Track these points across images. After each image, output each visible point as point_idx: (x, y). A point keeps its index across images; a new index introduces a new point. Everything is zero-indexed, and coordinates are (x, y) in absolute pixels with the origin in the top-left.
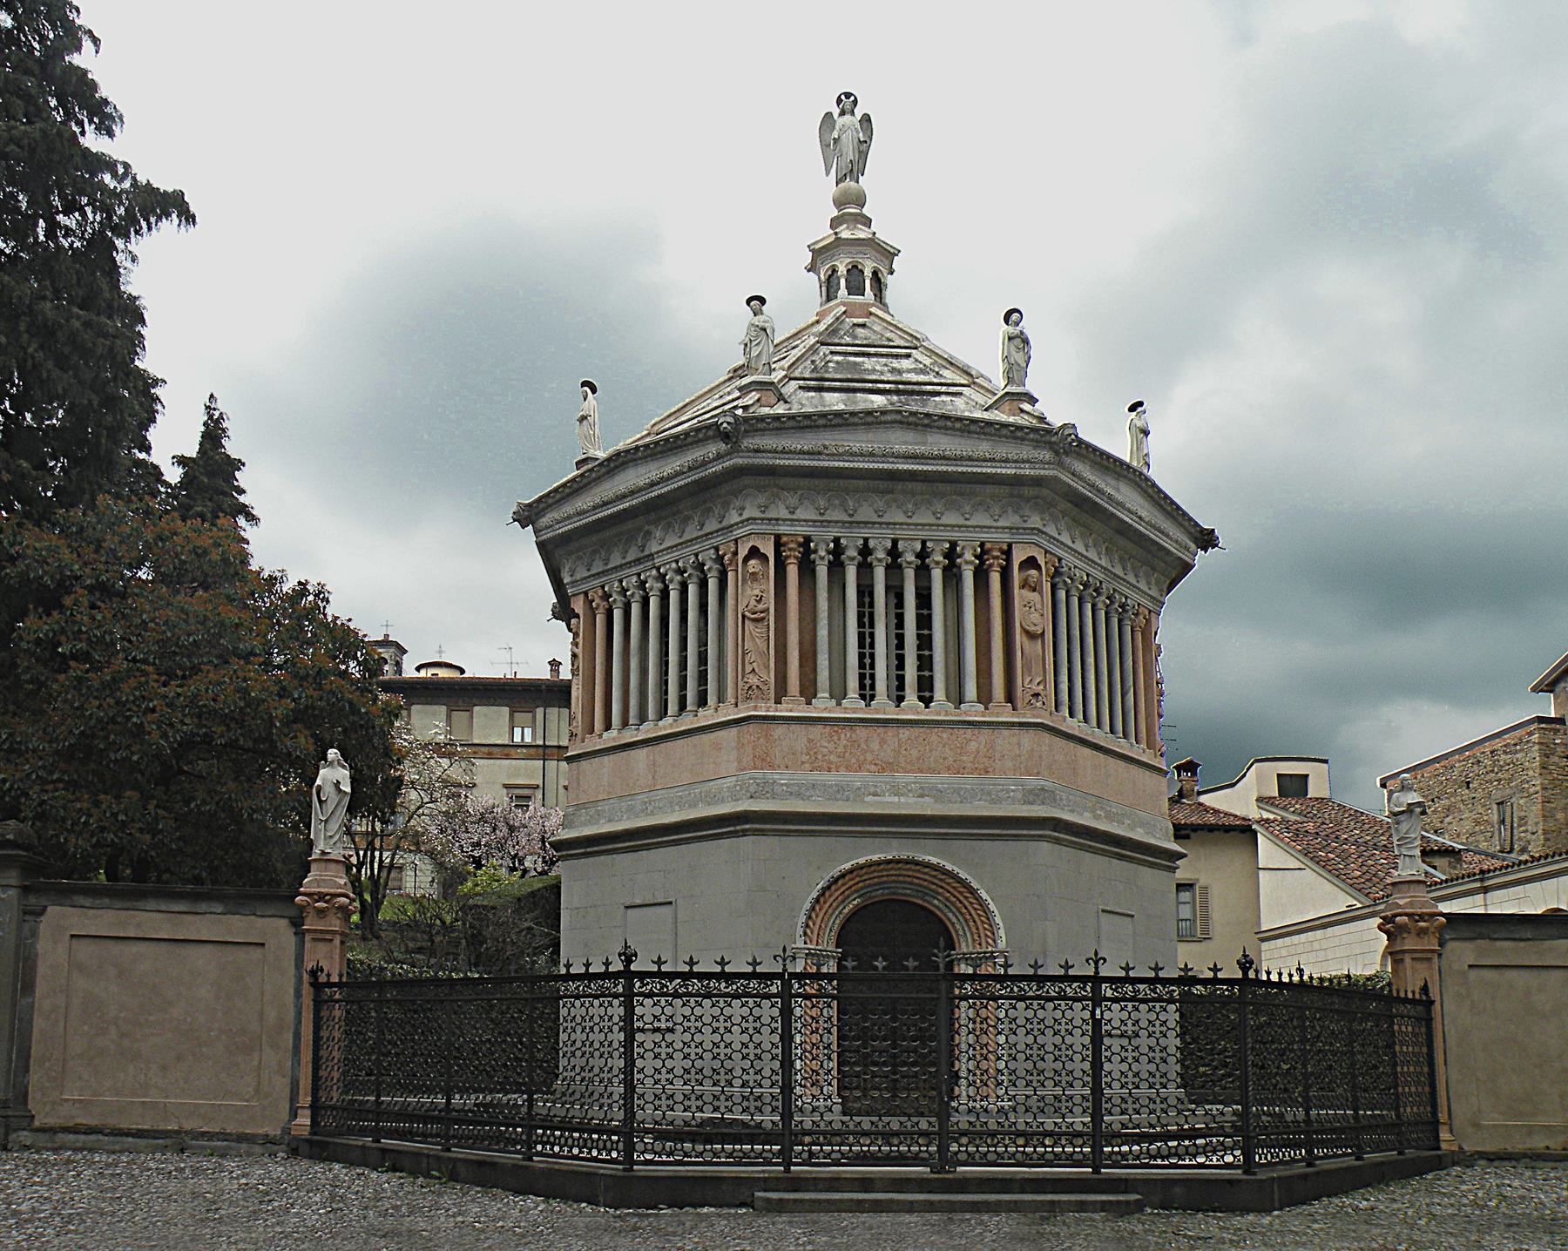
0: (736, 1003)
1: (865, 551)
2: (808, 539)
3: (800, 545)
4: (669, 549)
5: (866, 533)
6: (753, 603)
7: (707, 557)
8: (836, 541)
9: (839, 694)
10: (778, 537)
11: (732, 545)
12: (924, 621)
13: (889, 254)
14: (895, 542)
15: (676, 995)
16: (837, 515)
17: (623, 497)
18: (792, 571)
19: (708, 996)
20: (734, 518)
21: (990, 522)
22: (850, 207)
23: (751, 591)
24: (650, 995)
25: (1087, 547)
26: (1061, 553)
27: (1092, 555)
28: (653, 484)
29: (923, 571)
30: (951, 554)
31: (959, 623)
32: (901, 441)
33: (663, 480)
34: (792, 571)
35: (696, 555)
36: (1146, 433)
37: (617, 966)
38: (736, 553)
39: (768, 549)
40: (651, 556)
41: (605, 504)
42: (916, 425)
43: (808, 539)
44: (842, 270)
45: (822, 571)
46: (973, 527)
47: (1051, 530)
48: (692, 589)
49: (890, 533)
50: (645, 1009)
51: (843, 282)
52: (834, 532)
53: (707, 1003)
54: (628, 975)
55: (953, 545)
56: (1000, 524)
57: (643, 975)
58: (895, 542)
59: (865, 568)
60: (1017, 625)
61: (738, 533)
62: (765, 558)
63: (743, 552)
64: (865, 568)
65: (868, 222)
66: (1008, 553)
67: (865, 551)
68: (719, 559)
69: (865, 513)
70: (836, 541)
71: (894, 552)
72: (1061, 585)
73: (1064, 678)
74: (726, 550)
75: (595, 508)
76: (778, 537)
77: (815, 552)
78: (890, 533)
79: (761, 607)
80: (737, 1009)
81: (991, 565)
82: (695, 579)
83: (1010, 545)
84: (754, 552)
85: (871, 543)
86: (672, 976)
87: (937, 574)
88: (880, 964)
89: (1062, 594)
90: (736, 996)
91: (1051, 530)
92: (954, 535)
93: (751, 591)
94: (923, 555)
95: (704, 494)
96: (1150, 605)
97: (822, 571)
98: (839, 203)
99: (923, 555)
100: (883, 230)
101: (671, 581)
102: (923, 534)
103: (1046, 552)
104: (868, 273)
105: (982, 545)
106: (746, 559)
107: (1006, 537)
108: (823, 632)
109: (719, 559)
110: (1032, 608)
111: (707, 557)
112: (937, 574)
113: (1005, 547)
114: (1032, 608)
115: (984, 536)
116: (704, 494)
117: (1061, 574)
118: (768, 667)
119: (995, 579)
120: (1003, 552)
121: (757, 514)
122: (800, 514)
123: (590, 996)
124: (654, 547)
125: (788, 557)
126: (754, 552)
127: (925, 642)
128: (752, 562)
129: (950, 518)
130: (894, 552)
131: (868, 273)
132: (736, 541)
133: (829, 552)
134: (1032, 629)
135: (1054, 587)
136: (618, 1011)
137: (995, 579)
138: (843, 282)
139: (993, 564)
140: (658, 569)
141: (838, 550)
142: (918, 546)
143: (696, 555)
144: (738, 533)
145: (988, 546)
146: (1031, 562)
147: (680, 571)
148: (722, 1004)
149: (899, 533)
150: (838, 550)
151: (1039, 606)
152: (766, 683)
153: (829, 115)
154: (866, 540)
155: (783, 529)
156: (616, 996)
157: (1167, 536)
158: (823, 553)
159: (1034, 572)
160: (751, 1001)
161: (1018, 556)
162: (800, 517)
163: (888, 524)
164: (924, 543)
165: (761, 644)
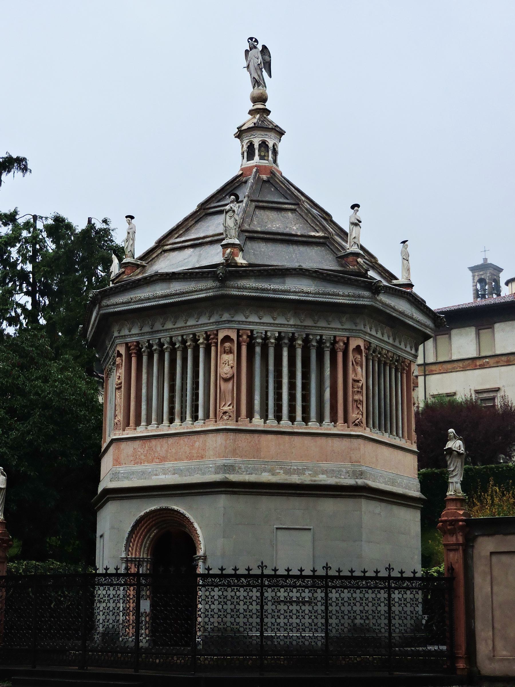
2: (138, 343)
5: (159, 335)
8: (148, 341)
10: (127, 344)
16: (146, 329)
18: (134, 360)
25: (274, 319)
26: (251, 327)
30: (195, 339)
34: (134, 360)
39: (122, 350)
45: (145, 359)
46: (199, 325)
52: (147, 337)
55: (194, 335)
56: (211, 321)
58: (171, 338)
76: (127, 344)
79: (119, 381)
83: (217, 331)
91: (240, 318)
94: (184, 342)
97: (145, 359)
98: (256, 100)
99: (184, 342)
102: (182, 332)
105: (206, 333)
117: (256, 338)
129: (191, 322)
134: (225, 376)
142: (180, 338)
145: (209, 333)
149: (173, 333)
150: (150, 346)
155: (128, 340)
157: (338, 295)
159: (227, 345)
164: (182, 336)
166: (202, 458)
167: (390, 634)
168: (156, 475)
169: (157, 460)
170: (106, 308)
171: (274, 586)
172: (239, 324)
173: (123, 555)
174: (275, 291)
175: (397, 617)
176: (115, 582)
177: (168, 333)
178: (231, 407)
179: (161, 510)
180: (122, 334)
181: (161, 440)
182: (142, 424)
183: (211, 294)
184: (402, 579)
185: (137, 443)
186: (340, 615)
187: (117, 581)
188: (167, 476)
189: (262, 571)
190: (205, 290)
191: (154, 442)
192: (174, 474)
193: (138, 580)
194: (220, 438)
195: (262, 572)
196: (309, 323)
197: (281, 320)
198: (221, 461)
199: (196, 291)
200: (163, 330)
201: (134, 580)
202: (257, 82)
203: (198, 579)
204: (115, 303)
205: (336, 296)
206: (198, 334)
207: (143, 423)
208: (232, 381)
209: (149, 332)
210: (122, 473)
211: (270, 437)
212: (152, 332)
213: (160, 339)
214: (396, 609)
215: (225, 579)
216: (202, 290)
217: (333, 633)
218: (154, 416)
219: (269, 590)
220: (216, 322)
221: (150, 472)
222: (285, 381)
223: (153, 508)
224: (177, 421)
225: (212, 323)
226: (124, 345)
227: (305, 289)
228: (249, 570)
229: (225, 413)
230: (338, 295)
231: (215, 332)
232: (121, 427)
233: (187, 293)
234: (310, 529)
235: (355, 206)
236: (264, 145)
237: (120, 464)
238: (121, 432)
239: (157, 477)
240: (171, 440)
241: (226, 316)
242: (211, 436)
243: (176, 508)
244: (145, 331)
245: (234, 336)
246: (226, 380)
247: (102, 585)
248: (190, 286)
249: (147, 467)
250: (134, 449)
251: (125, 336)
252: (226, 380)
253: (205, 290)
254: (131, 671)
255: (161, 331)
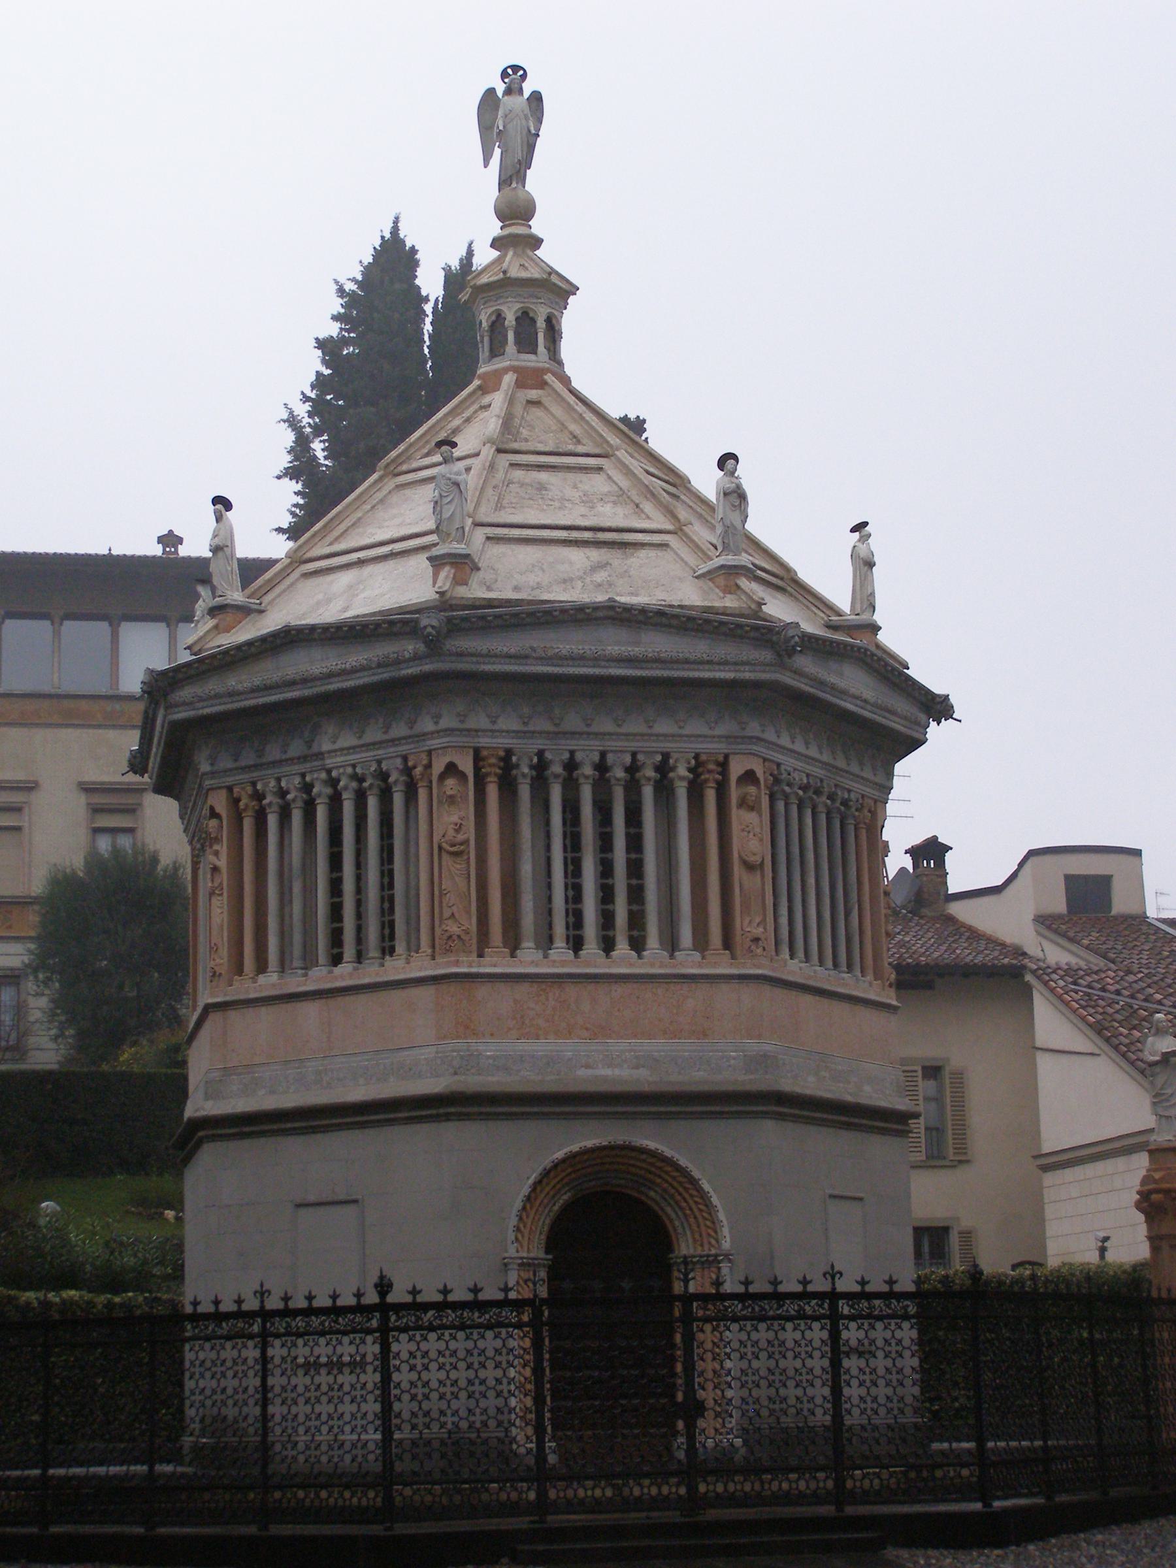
0: (489, 1334)
1: (571, 766)
2: (509, 752)
3: (501, 759)
4: (343, 749)
5: (573, 744)
6: (451, 833)
7: (393, 766)
9: (546, 942)
11: (424, 756)
12: (635, 843)
13: (559, 290)
14: (603, 755)
15: (431, 1328)
16: (542, 724)
17: (292, 684)
18: (492, 791)
19: (462, 1327)
20: (427, 725)
21: (705, 730)
22: (515, 211)
23: (450, 818)
24: (404, 1330)
25: (807, 744)
26: (778, 757)
27: (813, 752)
28: (330, 675)
29: (633, 787)
30: (664, 768)
31: (672, 850)
32: (615, 642)
33: (344, 673)
34: (492, 791)
35: (379, 762)
36: (870, 564)
37: (372, 1298)
38: (429, 766)
39: (466, 765)
40: (320, 755)
41: (267, 688)
42: (629, 620)
43: (509, 752)
44: (510, 319)
45: (524, 791)
46: (686, 736)
47: (770, 735)
48: (372, 803)
49: (597, 745)
50: (402, 1346)
51: (511, 336)
53: (461, 1335)
54: (384, 1308)
55: (666, 756)
56: (717, 732)
57: (398, 1307)
58: (603, 755)
59: (571, 785)
60: (736, 855)
61: (435, 743)
62: (463, 776)
63: (438, 767)
64: (571, 785)
65: (537, 242)
66: (724, 765)
67: (571, 766)
68: (408, 771)
69: (573, 721)
70: (540, 754)
71: (602, 767)
72: (779, 796)
73: (784, 911)
74: (418, 761)
75: (253, 691)
76: (477, 752)
77: (517, 766)
78: (597, 745)
79: (461, 837)
80: (489, 1342)
81: (706, 781)
82: (375, 791)
83: (726, 757)
84: (451, 769)
85: (579, 756)
86: (426, 1307)
87: (648, 792)
88: (626, 1285)
89: (780, 806)
90: (489, 1327)
92: (668, 746)
93: (450, 818)
95: (391, 695)
96: (876, 794)
97: (524, 791)
99: (633, 769)
100: (554, 254)
101: (346, 788)
102: (634, 745)
103: (765, 760)
104: (541, 324)
105: (697, 757)
106: (442, 777)
107: (720, 747)
108: (526, 868)
109: (408, 771)
110: (750, 832)
111: (393, 766)
112: (648, 792)
113: (721, 759)
114: (750, 832)
115: (700, 746)
116: (391, 695)
118: (468, 912)
119: (710, 796)
120: (719, 764)
121: (454, 724)
122: (502, 724)
123: (338, 1332)
124: (326, 747)
125: (488, 774)
126: (451, 769)
127: (635, 868)
128: (450, 782)
129: (664, 726)
130: (602, 767)
131: (541, 324)
132: (430, 753)
133: (532, 767)
134: (751, 859)
135: (772, 798)
136: (372, 1348)
137: (710, 796)
138: (511, 336)
139: (710, 777)
140: (329, 771)
141: (541, 766)
142: (628, 759)
143: (379, 762)
144: (435, 743)
146: (749, 777)
147: (361, 780)
148: (475, 1336)
150: (541, 766)
151: (758, 830)
152: (467, 932)
153: (491, 92)
154: (572, 753)
155: (484, 741)
156: (369, 1332)
158: (526, 770)
159: (752, 790)
160: (504, 1331)
161: (737, 769)
162: (503, 728)
163: (596, 734)
165: (461, 882)
166: (705, 1035)
167: (837, 1416)
168: (587, 1066)
169: (585, 1034)
170: (454, 658)
171: (862, 1317)
172: (768, 748)
173: (512, 1251)
174: (833, 688)
175: (855, 1383)
176: (771, 1313)
177: (597, 743)
178: (761, 929)
179: (610, 1148)
180: (471, 724)
181: (591, 987)
182: (525, 944)
183: (747, 675)
184: (287, 1313)
185: (523, 990)
186: (894, 1377)
187: (778, 1309)
188: (617, 1072)
189: (833, 1284)
190: (736, 664)
191: (571, 991)
192: (637, 1068)
193: (834, 1307)
194: (747, 995)
195: (834, 1288)
196: (841, 763)
197: (813, 752)
198: (753, 1046)
199: (709, 662)
200: (588, 734)
201: (821, 1306)
202: (514, 174)
203: (841, 1303)
204: (485, 652)
205: (889, 711)
206: (675, 756)
207: (528, 944)
208: (759, 873)
209: (548, 733)
210: (489, 1057)
211: (808, 999)
212: (557, 733)
213: (572, 753)
214: (402, 1377)
215: (766, 1304)
216: (726, 663)
217: (854, 1419)
218: (590, 929)
219: (853, 1325)
220: (727, 737)
221: (569, 1059)
222: (811, 881)
223: (590, 1143)
224: (622, 948)
225: (719, 737)
226: (471, 752)
227: (869, 694)
228: (805, 1282)
229: (756, 940)
230: (894, 713)
231: (721, 759)
232: (474, 947)
233: (687, 661)
234: (861, 1199)
235: (859, 527)
236: (525, 319)
237: (475, 1034)
238: (474, 957)
239: (590, 1072)
240: (619, 990)
241: (754, 728)
242: (724, 987)
243: (652, 1145)
244: (538, 728)
245: (760, 774)
246: (750, 867)
247: (735, 1319)
248: (699, 648)
249: (568, 1047)
250: (515, 1001)
251: (476, 731)
252: (750, 867)
253: (736, 664)
254: (827, 1510)
255: (581, 734)
